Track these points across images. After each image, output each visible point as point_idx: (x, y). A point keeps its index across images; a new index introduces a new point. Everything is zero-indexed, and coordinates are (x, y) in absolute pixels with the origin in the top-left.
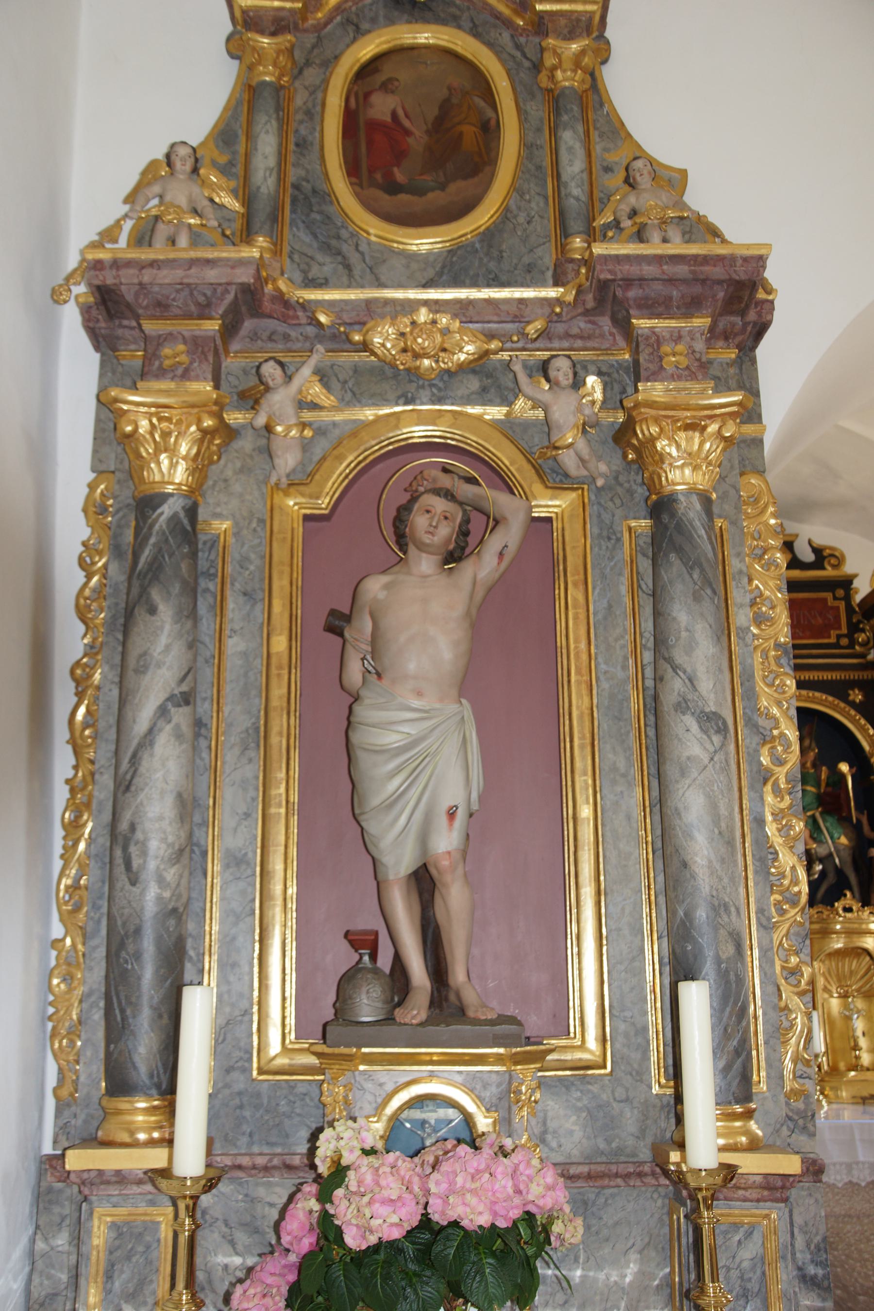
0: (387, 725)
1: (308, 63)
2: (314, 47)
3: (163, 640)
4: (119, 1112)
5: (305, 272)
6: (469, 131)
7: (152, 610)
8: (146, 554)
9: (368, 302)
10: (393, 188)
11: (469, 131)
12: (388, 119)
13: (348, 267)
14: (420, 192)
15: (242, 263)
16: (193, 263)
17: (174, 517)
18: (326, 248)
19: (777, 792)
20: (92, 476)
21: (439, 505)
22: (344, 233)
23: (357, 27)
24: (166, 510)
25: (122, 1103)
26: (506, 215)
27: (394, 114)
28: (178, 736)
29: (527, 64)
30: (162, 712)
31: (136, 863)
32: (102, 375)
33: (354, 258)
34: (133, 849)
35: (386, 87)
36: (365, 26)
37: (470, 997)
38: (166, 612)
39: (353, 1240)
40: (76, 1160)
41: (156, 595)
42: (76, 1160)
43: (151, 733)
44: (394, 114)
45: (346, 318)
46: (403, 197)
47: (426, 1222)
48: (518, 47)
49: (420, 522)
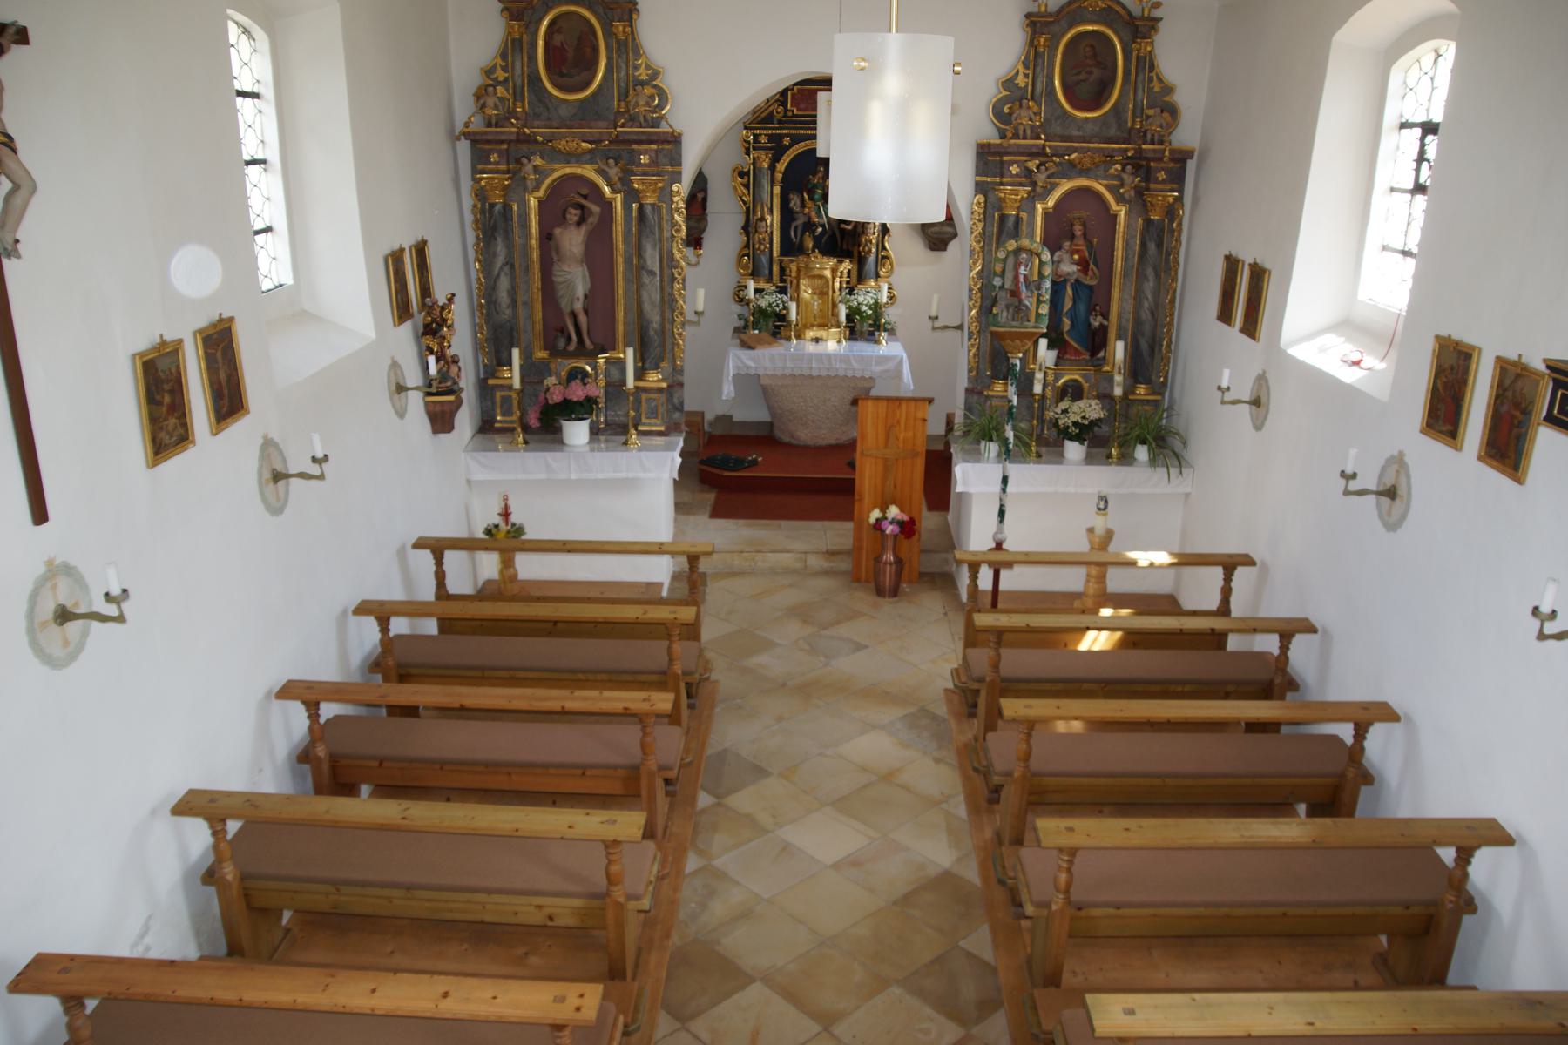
0: (560, 276)
1: (530, 22)
2: (532, 14)
3: (499, 248)
4: (499, 371)
5: (533, 111)
6: (588, 50)
7: (496, 239)
8: (492, 221)
9: (553, 133)
10: (562, 75)
11: (588, 50)
12: (559, 45)
13: (548, 109)
14: (571, 77)
15: (511, 133)
16: (497, 132)
17: (499, 211)
18: (540, 101)
19: (679, 284)
20: (472, 183)
21: (574, 211)
22: (546, 95)
23: (547, 5)
24: (497, 208)
25: (500, 368)
26: (600, 87)
27: (562, 43)
28: (506, 274)
29: (608, 21)
30: (501, 269)
31: (498, 309)
32: (472, 160)
33: (550, 106)
34: (497, 306)
35: (559, 31)
36: (550, 4)
37: (587, 342)
38: (499, 240)
39: (550, 402)
40: (491, 382)
41: (496, 235)
42: (491, 382)
43: (498, 276)
44: (562, 43)
45: (547, 138)
46: (565, 78)
47: (565, 399)
48: (605, 14)
49: (568, 216)
